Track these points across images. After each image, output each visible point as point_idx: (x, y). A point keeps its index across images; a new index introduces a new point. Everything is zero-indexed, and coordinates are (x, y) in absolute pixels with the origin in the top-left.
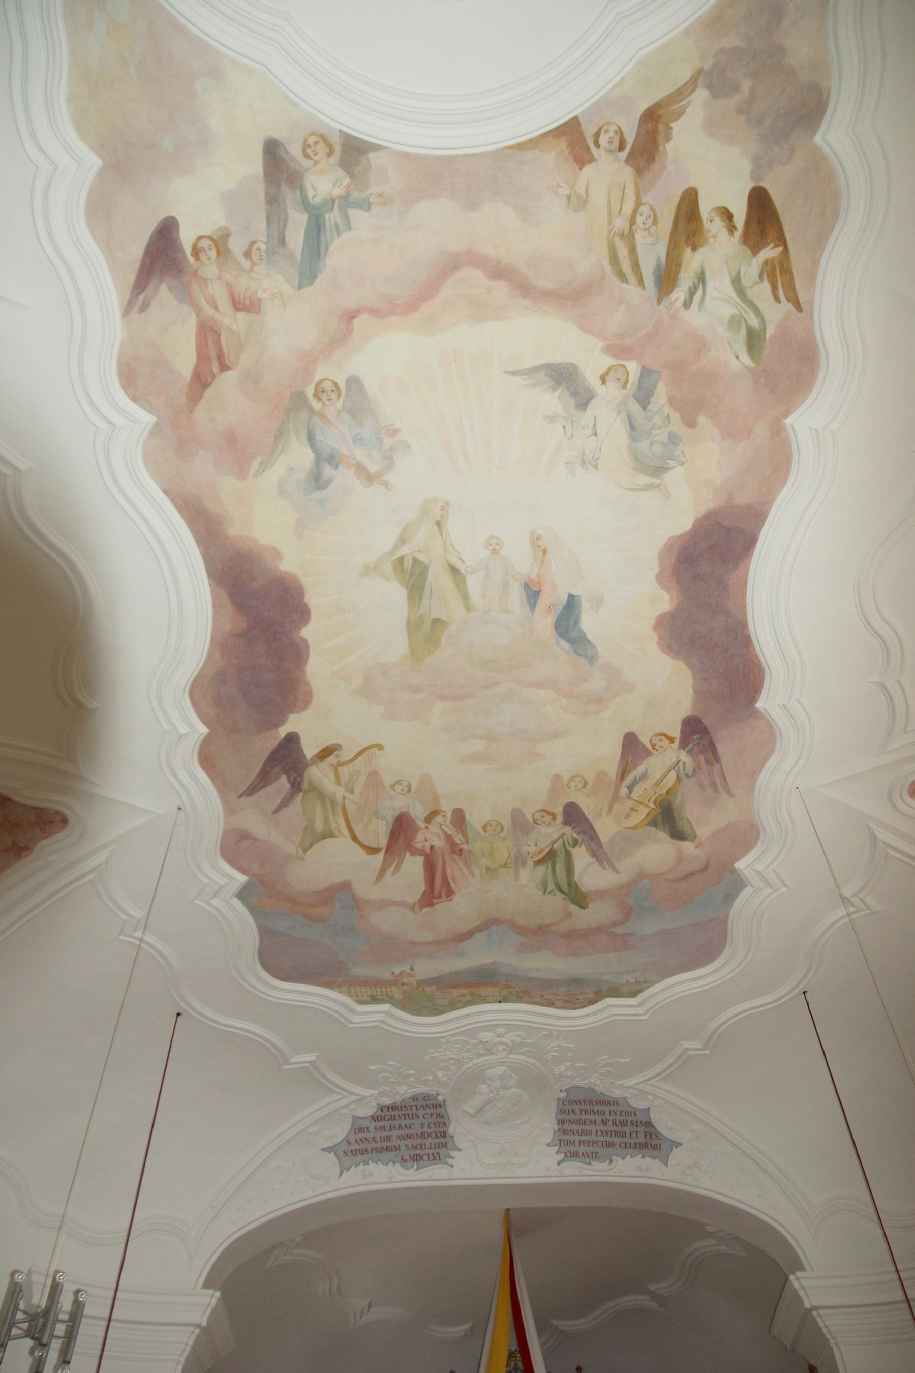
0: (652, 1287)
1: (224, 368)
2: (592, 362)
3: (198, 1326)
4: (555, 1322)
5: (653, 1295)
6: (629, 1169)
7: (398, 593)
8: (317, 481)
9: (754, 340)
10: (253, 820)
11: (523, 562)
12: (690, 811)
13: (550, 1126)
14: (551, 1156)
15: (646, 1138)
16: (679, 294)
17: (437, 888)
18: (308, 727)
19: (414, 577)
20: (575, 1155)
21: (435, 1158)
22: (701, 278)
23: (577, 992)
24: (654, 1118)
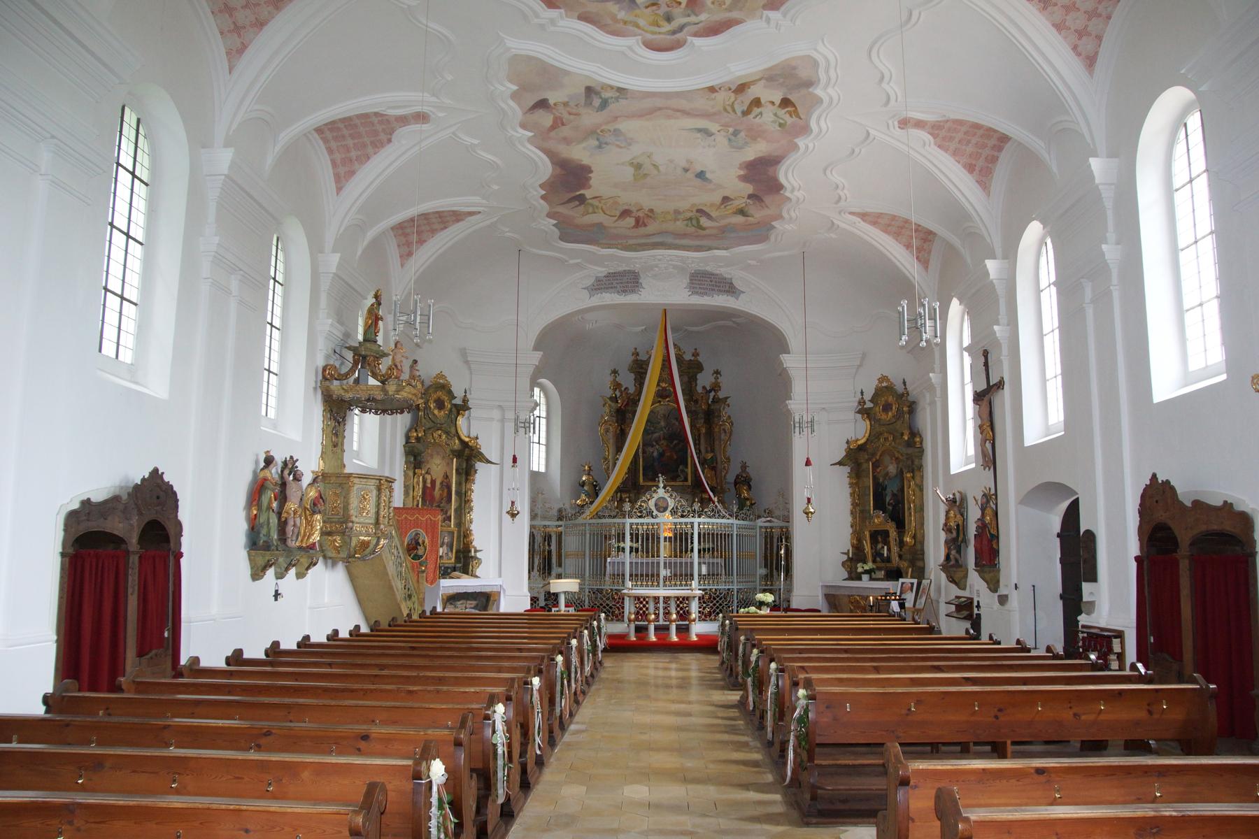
1: (563, 124)
2: (713, 127)
6: (720, 301)
7: (631, 170)
8: (600, 147)
9: (780, 125)
10: (561, 209)
11: (684, 164)
12: (751, 210)
13: (686, 281)
14: (687, 293)
15: (729, 288)
16: (751, 116)
17: (639, 223)
18: (588, 193)
19: (638, 167)
20: (697, 293)
21: (633, 292)
22: (761, 113)
23: (698, 249)
24: (734, 282)
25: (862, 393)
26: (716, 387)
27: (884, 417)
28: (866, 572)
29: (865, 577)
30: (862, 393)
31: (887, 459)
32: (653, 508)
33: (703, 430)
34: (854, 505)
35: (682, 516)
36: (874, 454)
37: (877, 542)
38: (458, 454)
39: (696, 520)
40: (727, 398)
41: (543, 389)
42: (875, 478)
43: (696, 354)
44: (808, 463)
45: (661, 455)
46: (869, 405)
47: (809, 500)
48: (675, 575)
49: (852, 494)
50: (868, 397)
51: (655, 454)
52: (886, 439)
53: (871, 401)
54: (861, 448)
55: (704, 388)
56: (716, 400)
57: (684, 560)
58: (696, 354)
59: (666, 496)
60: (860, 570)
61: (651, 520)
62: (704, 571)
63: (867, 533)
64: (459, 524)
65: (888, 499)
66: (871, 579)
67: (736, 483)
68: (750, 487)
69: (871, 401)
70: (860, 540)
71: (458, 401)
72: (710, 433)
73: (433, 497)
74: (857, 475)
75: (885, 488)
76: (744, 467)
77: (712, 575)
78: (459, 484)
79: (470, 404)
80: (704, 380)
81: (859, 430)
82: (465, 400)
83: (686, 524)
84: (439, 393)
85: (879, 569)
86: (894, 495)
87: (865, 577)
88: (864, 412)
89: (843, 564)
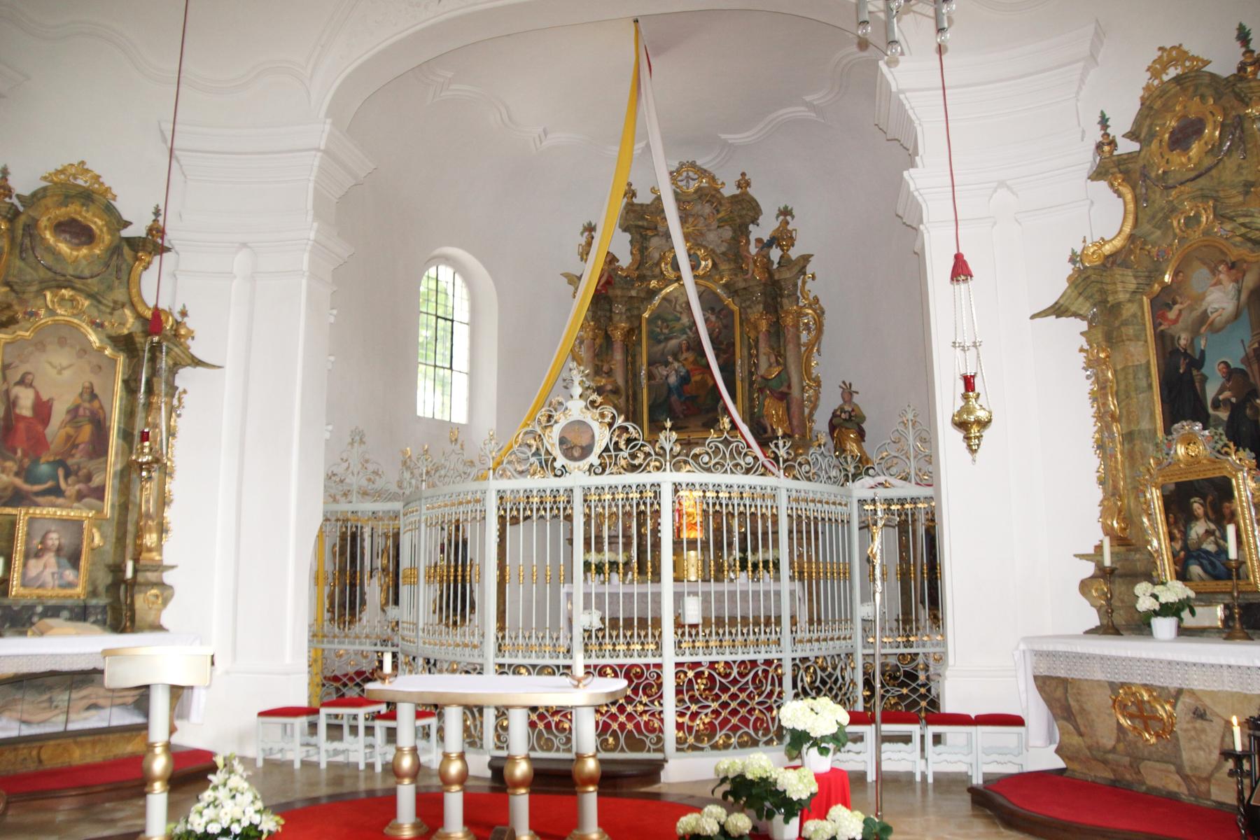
0: (808, 98)
3: (318, 150)
4: (724, 136)
5: (810, 106)
25: (1104, 122)
26: (782, 238)
27: (1177, 159)
28: (1167, 610)
29: (1164, 627)
30: (1104, 122)
31: (1199, 275)
32: (557, 452)
33: (763, 326)
34: (1104, 418)
35: (633, 468)
36: (1154, 273)
37: (1191, 517)
38: (126, 344)
39: (667, 478)
40: (806, 259)
41: (458, 267)
42: (1163, 340)
43: (744, 183)
44: (960, 270)
45: (684, 380)
46: (1127, 147)
47: (969, 382)
48: (614, 623)
49: (1099, 395)
50: (1121, 125)
51: (673, 379)
52: (1192, 221)
53: (1132, 135)
54: (1113, 261)
55: (759, 240)
56: (785, 261)
57: (726, 587)
58: (744, 183)
59: (591, 418)
60: (1145, 604)
61: (550, 483)
62: (693, 612)
63: (1154, 496)
64: (124, 507)
65: (1211, 390)
66: (1184, 632)
67: (832, 427)
68: (861, 435)
69: (1132, 135)
70: (1129, 519)
71: (137, 230)
72: (777, 331)
73: (38, 444)
74: (1107, 329)
75: (1198, 363)
76: (848, 392)
77: (717, 623)
78: (129, 414)
79: (172, 236)
80: (763, 229)
81: (1104, 218)
82: (157, 231)
83: (641, 489)
84: (73, 210)
85: (1206, 598)
86: (1230, 373)
87: (1164, 627)
88: (1110, 167)
89: (1084, 586)
